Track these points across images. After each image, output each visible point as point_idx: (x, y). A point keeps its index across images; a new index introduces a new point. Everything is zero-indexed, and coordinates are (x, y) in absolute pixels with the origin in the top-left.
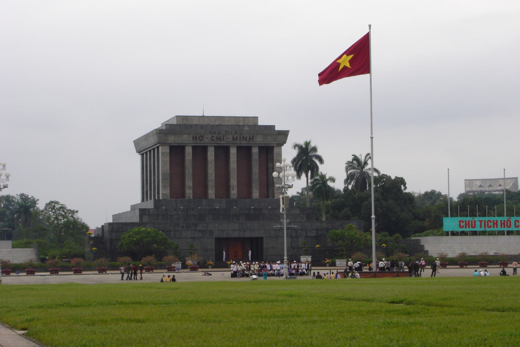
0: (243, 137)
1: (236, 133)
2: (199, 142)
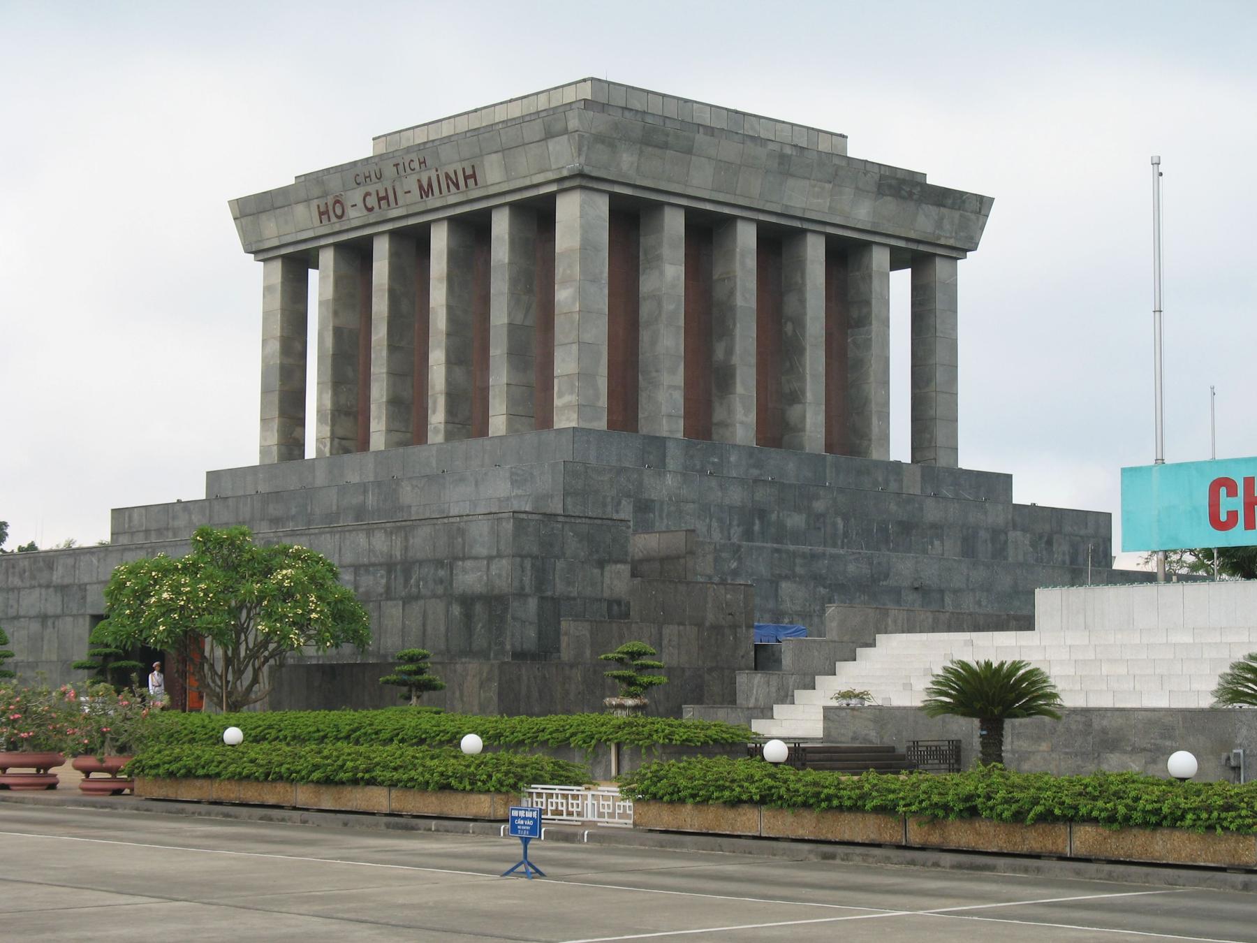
0: (447, 176)
1: (423, 163)
2: (337, 228)
